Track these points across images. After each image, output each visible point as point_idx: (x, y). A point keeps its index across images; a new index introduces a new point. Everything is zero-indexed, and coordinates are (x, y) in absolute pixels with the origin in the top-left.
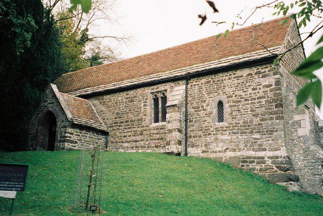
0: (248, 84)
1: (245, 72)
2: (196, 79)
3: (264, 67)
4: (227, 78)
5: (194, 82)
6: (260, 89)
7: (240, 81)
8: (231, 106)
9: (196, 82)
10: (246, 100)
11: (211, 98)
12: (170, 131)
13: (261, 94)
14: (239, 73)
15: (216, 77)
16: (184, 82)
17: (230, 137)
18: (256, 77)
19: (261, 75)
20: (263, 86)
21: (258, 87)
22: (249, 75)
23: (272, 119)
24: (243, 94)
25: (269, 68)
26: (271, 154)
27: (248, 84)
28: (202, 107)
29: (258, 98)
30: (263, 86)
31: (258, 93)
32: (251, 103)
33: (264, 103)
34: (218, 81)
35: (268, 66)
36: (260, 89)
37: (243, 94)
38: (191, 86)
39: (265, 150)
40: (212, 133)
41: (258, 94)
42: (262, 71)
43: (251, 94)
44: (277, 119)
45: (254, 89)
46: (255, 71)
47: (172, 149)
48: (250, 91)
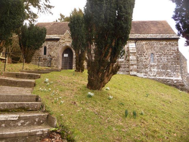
0: (165, 48)
1: (164, 43)
2: (140, 41)
3: (173, 42)
4: (156, 43)
5: (139, 42)
6: (171, 51)
7: (162, 46)
8: (157, 56)
9: (140, 43)
10: (165, 55)
11: (148, 51)
12: (132, 65)
13: (172, 53)
14: (161, 42)
15: (151, 42)
16: (134, 41)
17: (157, 70)
18: (169, 45)
19: (171, 45)
20: (172, 50)
21: (170, 50)
22: (166, 44)
23: (176, 64)
24: (163, 52)
25: (175, 43)
26: (176, 79)
27: (165, 48)
28: (143, 55)
29: (170, 55)
30: (172, 50)
31: (170, 52)
32: (167, 57)
33: (172, 57)
34: (151, 44)
35: (174, 42)
36: (171, 51)
37: (163, 52)
38: (138, 44)
39: (172, 77)
40: (148, 67)
41: (170, 53)
42: (172, 43)
43: (166, 52)
44: (178, 64)
45: (168, 51)
46: (169, 43)
47: (134, 73)
48: (166, 51)
